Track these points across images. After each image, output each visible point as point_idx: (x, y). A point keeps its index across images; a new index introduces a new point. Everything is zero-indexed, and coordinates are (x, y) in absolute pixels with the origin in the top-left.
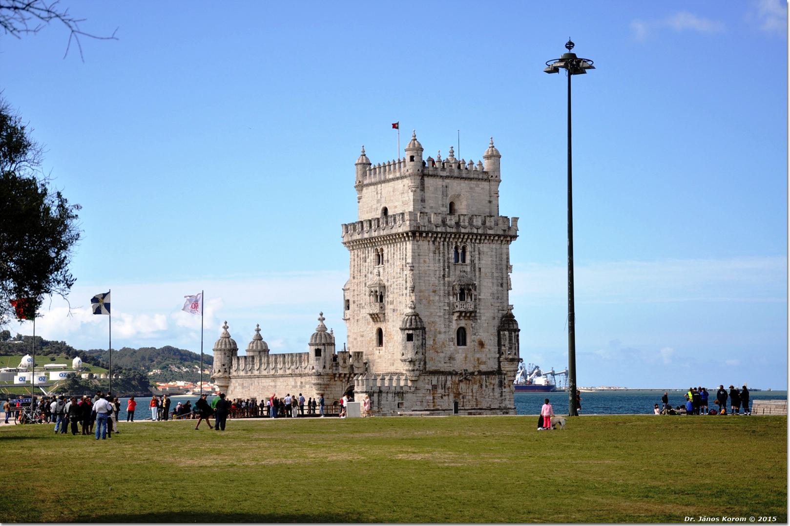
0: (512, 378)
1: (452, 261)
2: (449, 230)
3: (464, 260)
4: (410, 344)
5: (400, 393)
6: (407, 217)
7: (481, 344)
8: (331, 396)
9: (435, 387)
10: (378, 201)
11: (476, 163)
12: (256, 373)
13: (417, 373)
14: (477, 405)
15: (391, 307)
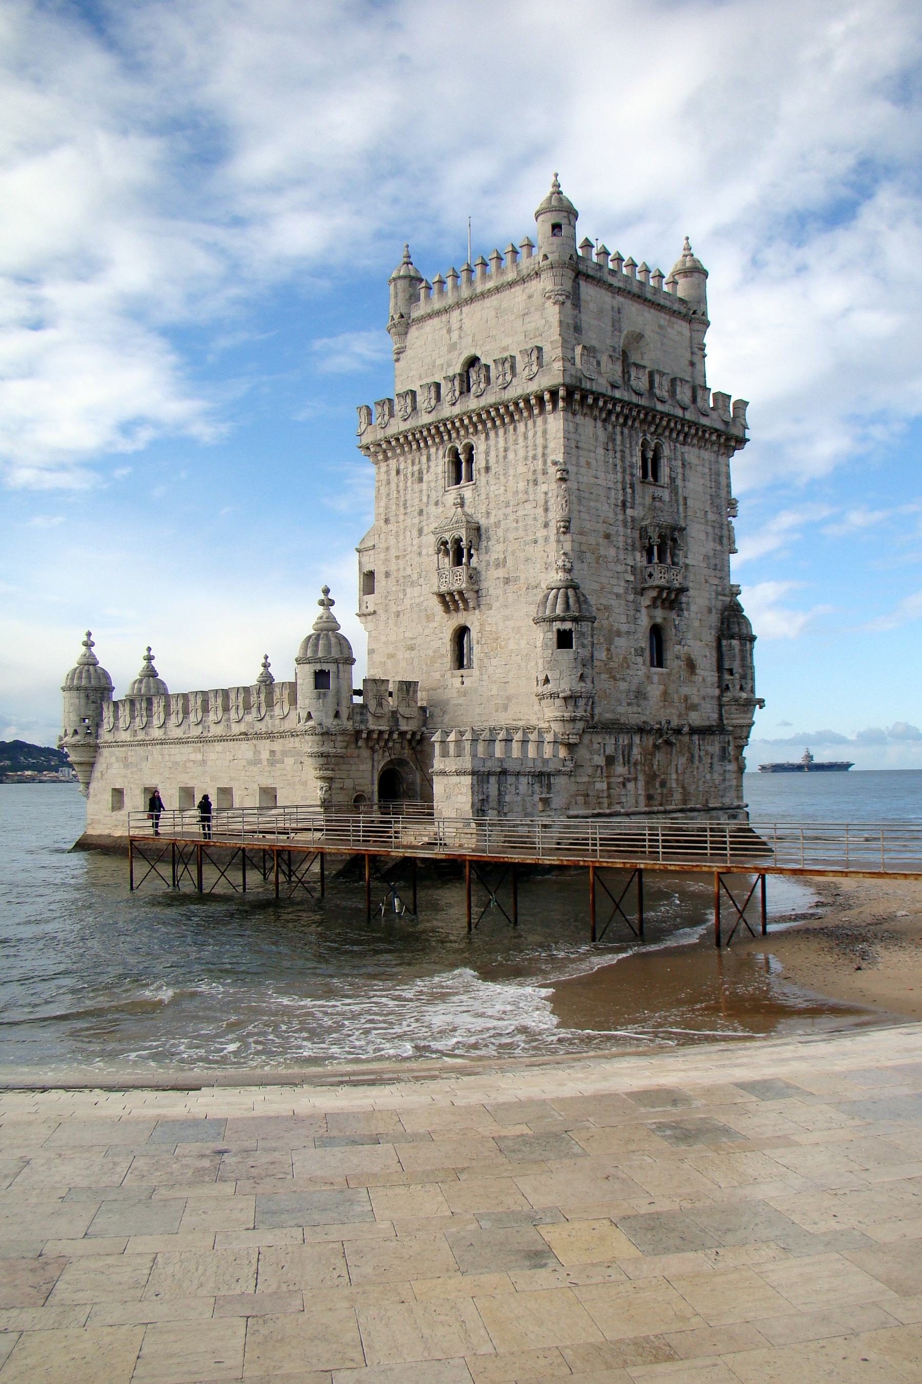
0: (741, 742)
1: (639, 473)
2: (635, 399)
3: (655, 476)
4: (566, 655)
5: (542, 777)
6: (553, 352)
7: (691, 666)
8: (349, 784)
9: (610, 760)
10: (452, 347)
11: (667, 274)
12: (156, 733)
13: (580, 725)
14: (685, 801)
15: (501, 573)
